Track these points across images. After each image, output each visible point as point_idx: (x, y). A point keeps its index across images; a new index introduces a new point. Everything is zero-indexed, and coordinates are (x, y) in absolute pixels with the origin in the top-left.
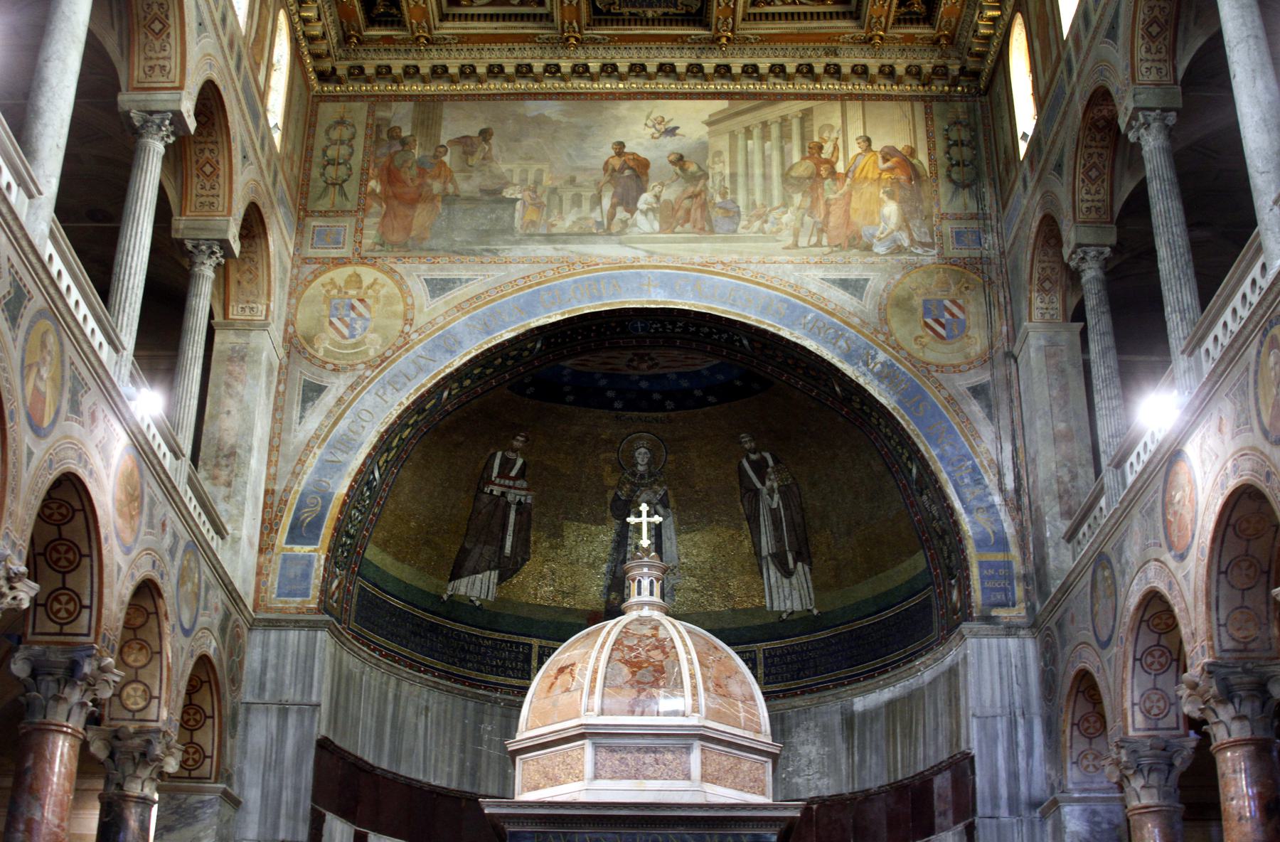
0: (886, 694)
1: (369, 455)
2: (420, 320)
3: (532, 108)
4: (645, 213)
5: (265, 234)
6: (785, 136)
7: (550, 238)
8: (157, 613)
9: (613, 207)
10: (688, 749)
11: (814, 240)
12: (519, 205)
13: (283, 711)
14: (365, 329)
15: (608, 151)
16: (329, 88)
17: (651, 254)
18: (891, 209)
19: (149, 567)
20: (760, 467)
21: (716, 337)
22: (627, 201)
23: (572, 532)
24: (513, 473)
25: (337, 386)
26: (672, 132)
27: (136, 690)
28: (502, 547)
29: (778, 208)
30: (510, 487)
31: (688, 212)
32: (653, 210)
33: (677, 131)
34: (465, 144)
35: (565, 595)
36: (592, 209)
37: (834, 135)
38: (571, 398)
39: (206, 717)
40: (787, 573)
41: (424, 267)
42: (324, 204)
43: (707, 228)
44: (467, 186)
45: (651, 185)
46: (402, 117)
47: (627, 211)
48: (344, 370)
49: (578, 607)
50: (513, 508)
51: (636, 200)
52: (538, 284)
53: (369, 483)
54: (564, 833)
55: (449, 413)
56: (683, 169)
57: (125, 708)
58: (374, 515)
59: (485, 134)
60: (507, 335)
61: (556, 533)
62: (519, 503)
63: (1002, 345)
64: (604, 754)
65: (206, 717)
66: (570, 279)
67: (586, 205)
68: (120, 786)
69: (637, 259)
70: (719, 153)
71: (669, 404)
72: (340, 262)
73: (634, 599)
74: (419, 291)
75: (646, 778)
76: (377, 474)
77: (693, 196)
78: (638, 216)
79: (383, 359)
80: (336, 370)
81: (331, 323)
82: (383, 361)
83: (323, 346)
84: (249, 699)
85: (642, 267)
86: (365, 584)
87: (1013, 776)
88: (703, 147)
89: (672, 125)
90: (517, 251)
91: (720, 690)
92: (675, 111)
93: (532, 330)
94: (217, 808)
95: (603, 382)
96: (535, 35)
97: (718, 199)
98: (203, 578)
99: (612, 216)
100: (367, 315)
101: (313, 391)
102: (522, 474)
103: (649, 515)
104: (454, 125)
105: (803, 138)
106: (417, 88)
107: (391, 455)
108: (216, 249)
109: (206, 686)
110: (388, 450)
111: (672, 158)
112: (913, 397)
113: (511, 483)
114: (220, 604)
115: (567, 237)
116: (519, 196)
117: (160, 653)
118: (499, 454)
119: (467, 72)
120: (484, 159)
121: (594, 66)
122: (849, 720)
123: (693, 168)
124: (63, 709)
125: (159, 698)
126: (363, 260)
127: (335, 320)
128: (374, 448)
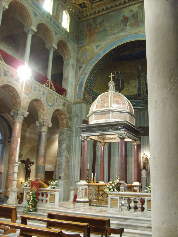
1: (89, 75)
2: (95, 52)
3: (110, 14)
4: (128, 26)
5: (67, 45)
7: (113, 34)
8: (42, 104)
9: (123, 26)
10: (109, 113)
12: (109, 30)
13: (78, 117)
14: (87, 56)
15: (122, 17)
16: (80, 20)
17: (129, 33)
19: (36, 97)
21: (142, 44)
22: (125, 25)
23: (131, 82)
24: (119, 74)
25: (84, 66)
26: (132, 11)
27: (42, 115)
28: (119, 86)
30: (119, 77)
31: (135, 24)
32: (129, 25)
33: (133, 11)
34: (100, 23)
35: (131, 92)
36: (120, 28)
38: (125, 60)
39: (64, 119)
41: (95, 44)
44: (101, 30)
45: (129, 21)
46: (91, 22)
48: (85, 63)
49: (133, 94)
50: (120, 80)
51: (127, 25)
52: (112, 42)
53: (91, 80)
54: (90, 130)
55: (103, 66)
56: (134, 17)
57: (41, 118)
58: (93, 84)
59: (103, 20)
60: (108, 52)
61: (128, 83)
62: (121, 79)
64: (96, 116)
65: (64, 119)
66: (117, 40)
68: (41, 130)
69: (127, 34)
70: (140, 12)
71: (141, 58)
73: (109, 89)
74: (95, 48)
75: (103, 119)
76: (92, 78)
77: (137, 20)
78: (127, 27)
79: (90, 60)
80: (84, 63)
81: (83, 56)
82: (90, 60)
83: (82, 60)
84: (73, 115)
85: (128, 35)
86: (94, 95)
88: (137, 12)
89: (132, 10)
90: (109, 38)
91: (117, 103)
92: (132, 8)
93: (111, 50)
94: (66, 132)
95: (129, 56)
96: (107, 2)
97: (140, 20)
98: (55, 98)
99: (123, 28)
100: (87, 54)
101: (81, 67)
102: (120, 74)
103: (112, 75)
104: (99, 20)
106: (92, 16)
107: (94, 75)
108: (52, 48)
109: (62, 114)
110: (93, 74)
111: (132, 15)
113: (119, 76)
114: (62, 101)
115: (116, 33)
116: (108, 29)
117: (44, 109)
118: (116, 72)
119: (99, 12)
120: (103, 24)
121: (118, 4)
123: (136, 16)
124: (17, 119)
125: (45, 116)
126: (87, 45)
127: (83, 56)
128: (90, 74)
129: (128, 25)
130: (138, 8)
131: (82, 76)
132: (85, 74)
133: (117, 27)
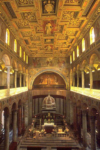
0: (62, 91)
18: (63, 64)
20: (55, 77)
25: (32, 76)
42: (30, 65)
43: (52, 66)
59: (39, 60)
63: (69, 73)
72: (31, 68)
83: (31, 74)
87: (68, 98)
105: (58, 60)
112: (64, 76)
122: (60, 91)
126: (33, 68)
131: (31, 80)
132: (33, 80)
133: (45, 64)
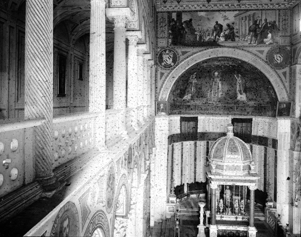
4: (222, 37)
6: (250, 20)
9: (216, 36)
11: (254, 42)
26: (227, 19)
29: (247, 35)
32: (224, 36)
36: (212, 36)
37: (260, 19)
40: (241, 94)
47: (218, 36)
56: (229, 27)
67: (210, 36)
77: (231, 33)
78: (221, 38)
111: (227, 25)
116: (198, 34)
129: (221, 35)
130: (235, 17)
